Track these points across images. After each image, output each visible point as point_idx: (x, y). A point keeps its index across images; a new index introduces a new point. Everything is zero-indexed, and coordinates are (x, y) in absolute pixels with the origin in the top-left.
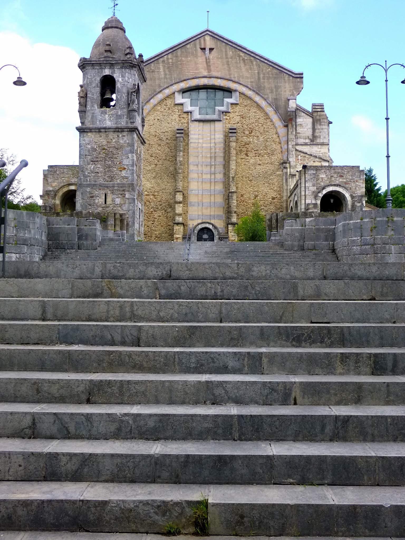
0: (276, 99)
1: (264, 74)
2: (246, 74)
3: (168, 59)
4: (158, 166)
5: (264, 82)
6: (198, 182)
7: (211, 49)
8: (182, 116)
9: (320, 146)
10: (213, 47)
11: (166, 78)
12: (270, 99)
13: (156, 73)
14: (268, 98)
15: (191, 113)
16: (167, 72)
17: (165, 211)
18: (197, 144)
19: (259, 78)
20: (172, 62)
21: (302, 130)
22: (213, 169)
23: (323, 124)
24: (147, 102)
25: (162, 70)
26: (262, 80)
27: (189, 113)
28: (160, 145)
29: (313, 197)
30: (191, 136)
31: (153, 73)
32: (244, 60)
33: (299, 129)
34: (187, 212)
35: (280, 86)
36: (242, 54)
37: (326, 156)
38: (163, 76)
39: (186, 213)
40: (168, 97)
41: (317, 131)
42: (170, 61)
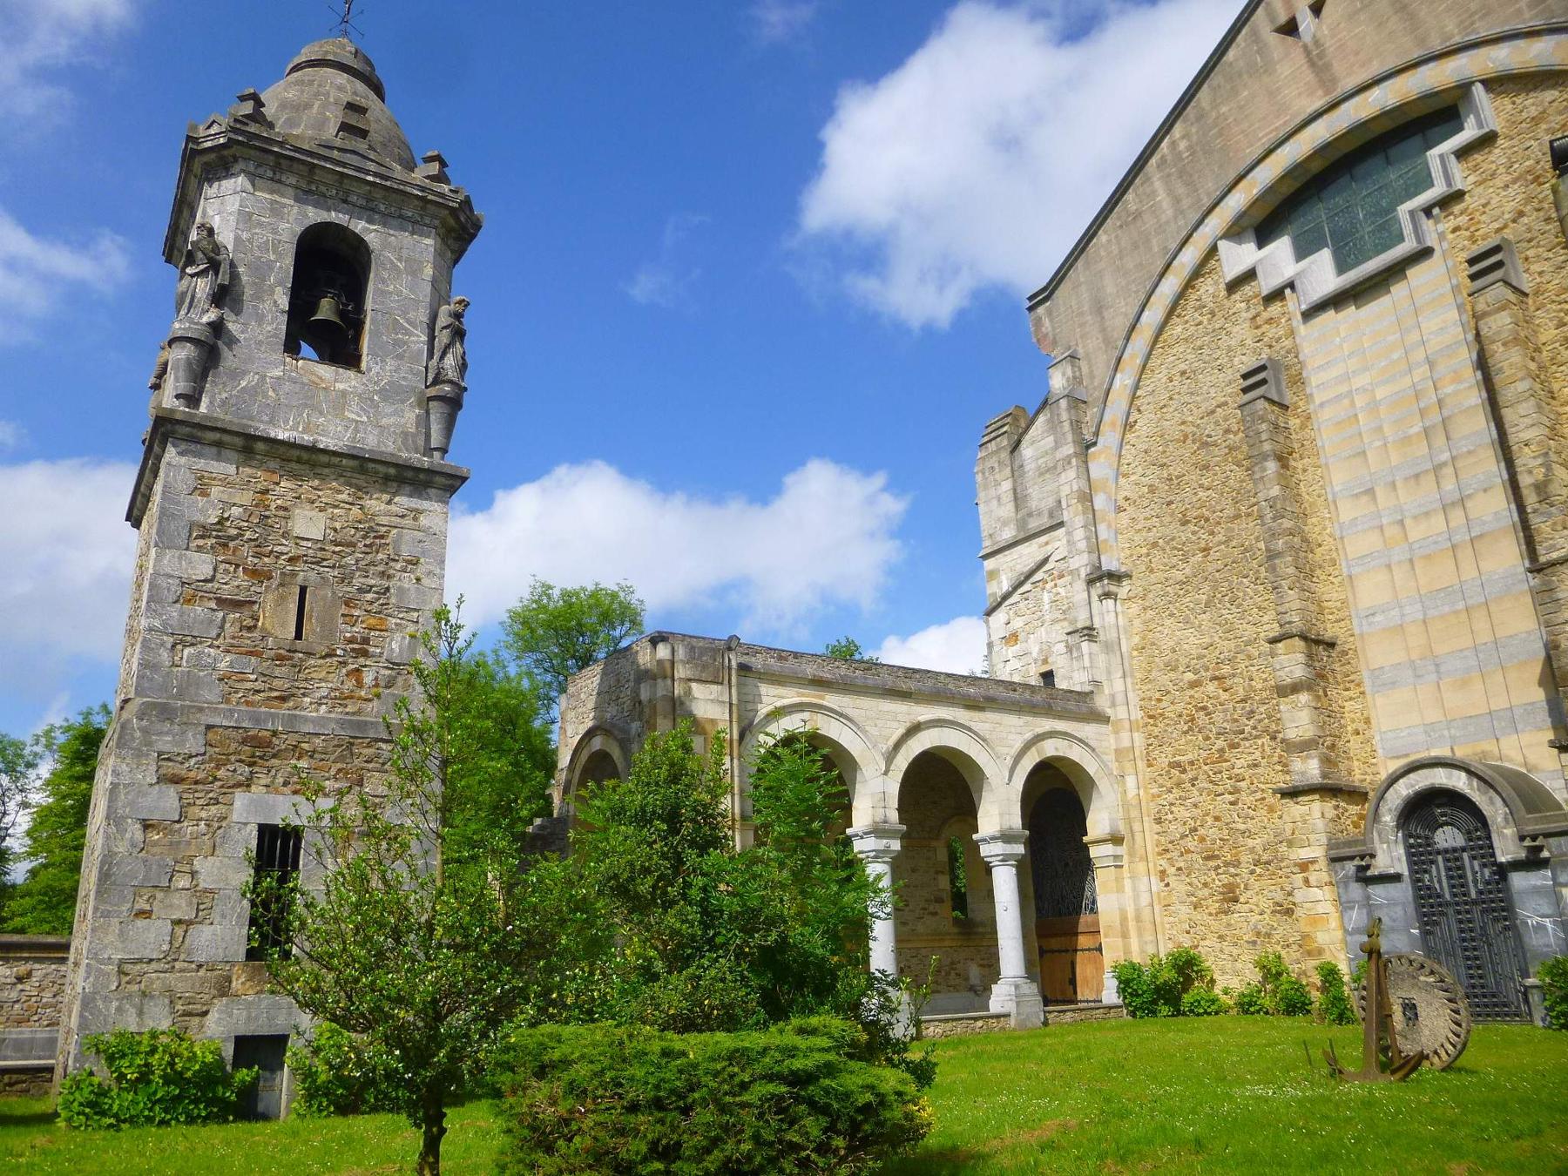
3: (1173, 144)
4: (1213, 555)
6: (1389, 566)
8: (1265, 315)
11: (1182, 212)
13: (1146, 217)
15: (1291, 285)
16: (1181, 190)
17: (1274, 738)
18: (1346, 402)
20: (1189, 148)
22: (1449, 485)
24: (1133, 328)
27: (1288, 291)
28: (1206, 467)
30: (1314, 380)
31: (1139, 223)
34: (1367, 721)
38: (1170, 212)
39: (1361, 726)
40: (1197, 273)
42: (1182, 145)
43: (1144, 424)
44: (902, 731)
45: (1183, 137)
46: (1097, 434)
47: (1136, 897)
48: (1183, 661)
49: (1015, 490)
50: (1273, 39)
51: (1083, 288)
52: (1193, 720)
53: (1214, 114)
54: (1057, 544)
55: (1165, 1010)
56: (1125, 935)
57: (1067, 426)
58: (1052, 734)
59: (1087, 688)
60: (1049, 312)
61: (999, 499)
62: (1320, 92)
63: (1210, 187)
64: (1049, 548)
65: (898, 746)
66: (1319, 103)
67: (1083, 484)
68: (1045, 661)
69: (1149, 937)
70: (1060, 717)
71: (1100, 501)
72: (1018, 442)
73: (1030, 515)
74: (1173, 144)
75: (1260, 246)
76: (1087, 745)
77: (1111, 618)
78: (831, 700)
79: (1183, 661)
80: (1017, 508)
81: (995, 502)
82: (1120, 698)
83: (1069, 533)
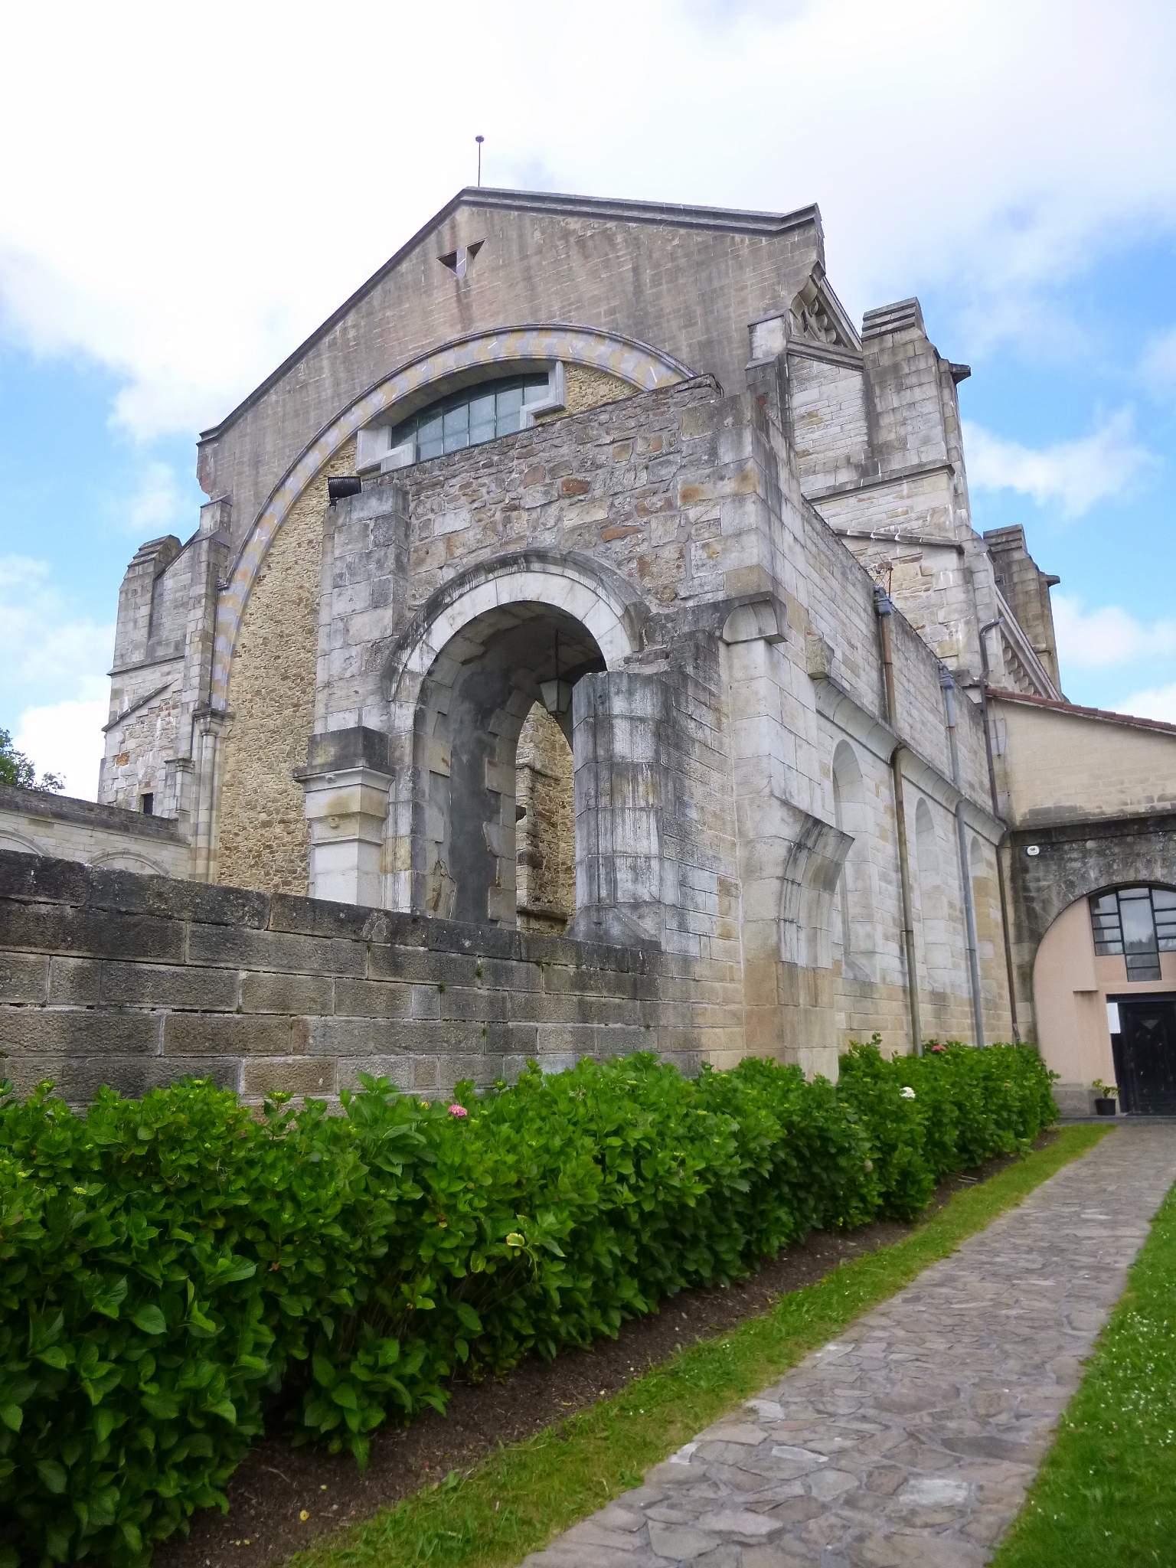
0: (708, 345)
1: (657, 266)
2: (590, 289)
3: (345, 330)
5: (658, 296)
7: (474, 250)
9: (905, 487)
10: (478, 240)
11: (339, 395)
12: (685, 350)
14: (678, 349)
16: (342, 375)
19: (638, 289)
20: (355, 338)
21: (815, 436)
23: (913, 380)
24: (277, 490)
25: (326, 373)
26: (649, 292)
29: (371, 683)
32: (581, 242)
33: (804, 438)
35: (722, 288)
36: (574, 224)
37: (941, 527)
38: (329, 392)
41: (886, 420)
42: (352, 334)
43: (272, 579)
45: (354, 326)
46: (229, 581)
48: (262, 802)
49: (151, 616)
50: (437, 265)
51: (247, 439)
52: (259, 856)
53: (380, 316)
54: (177, 676)
57: (204, 566)
59: (174, 816)
60: (215, 453)
61: (136, 622)
62: (459, 327)
63: (365, 380)
64: (170, 677)
66: (454, 336)
67: (209, 623)
68: (148, 784)
71: (221, 644)
72: (163, 572)
73: (159, 643)
74: (345, 330)
75: (393, 445)
77: (207, 754)
79: (262, 802)
80: (150, 634)
81: (132, 624)
82: (202, 828)
83: (187, 668)
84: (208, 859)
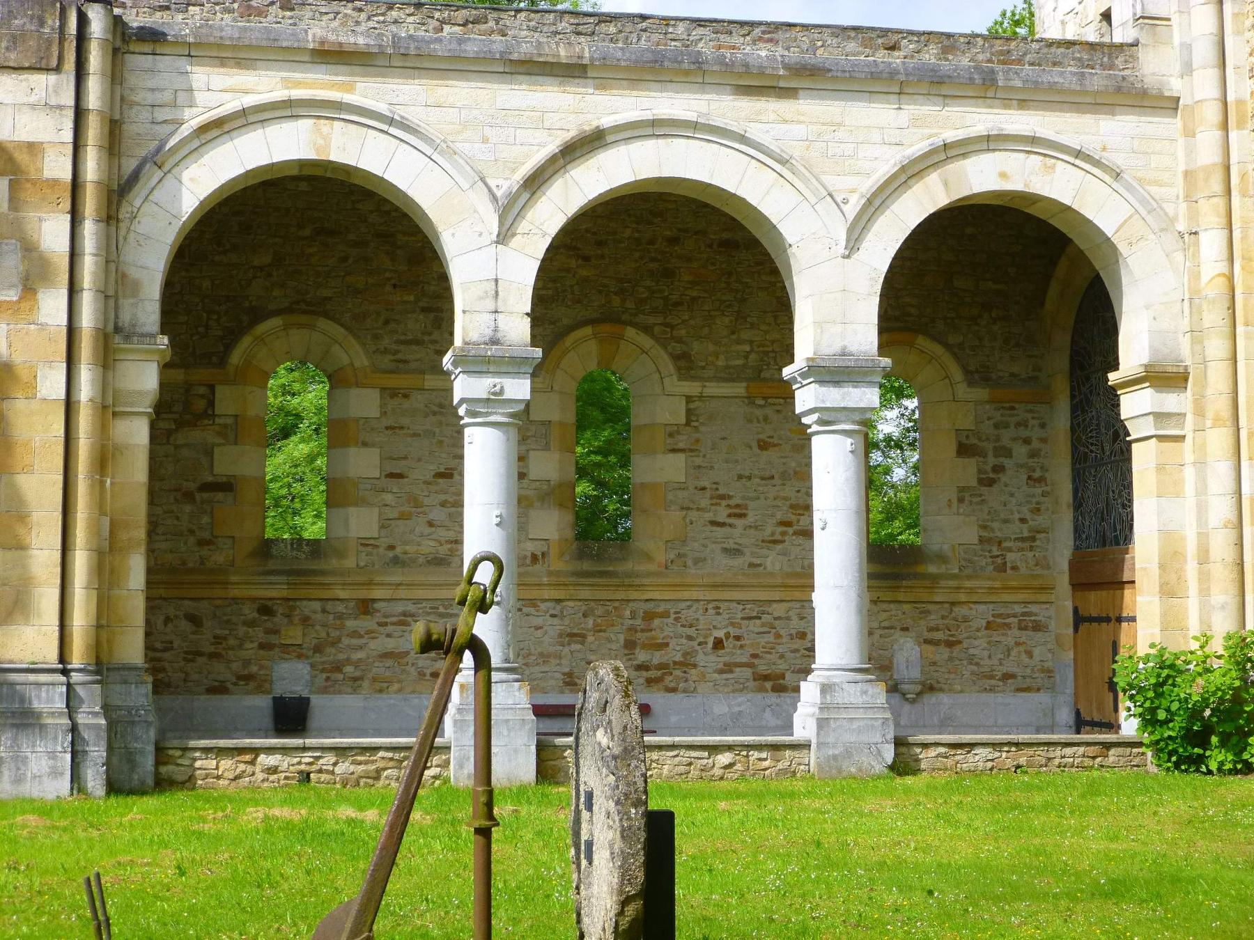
44: (552, 147)
47: (1201, 509)
55: (1218, 757)
56: (1169, 591)
58: (991, 142)
65: (536, 182)
69: (1222, 595)
70: (1023, 104)
76: (1097, 163)
78: (369, 92)
84: (1225, 126)
